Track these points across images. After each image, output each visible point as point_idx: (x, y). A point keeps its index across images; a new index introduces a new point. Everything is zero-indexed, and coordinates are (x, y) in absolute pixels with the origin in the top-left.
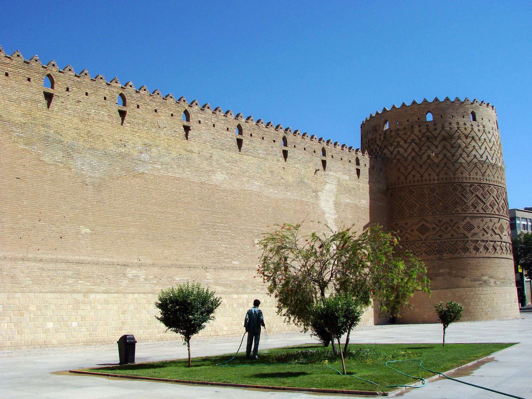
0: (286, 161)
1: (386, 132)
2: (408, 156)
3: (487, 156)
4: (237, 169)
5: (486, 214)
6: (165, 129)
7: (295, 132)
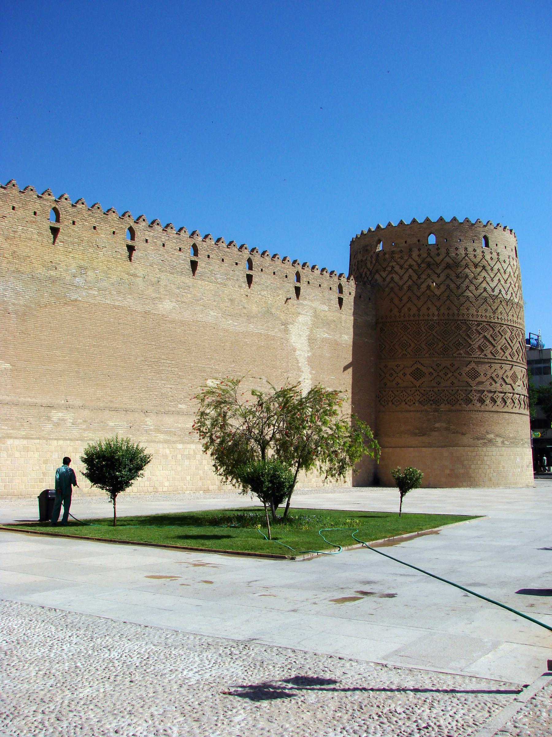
0: (249, 287)
3: (500, 290)
4: (189, 296)
5: (495, 359)
6: (105, 249)
7: (264, 253)
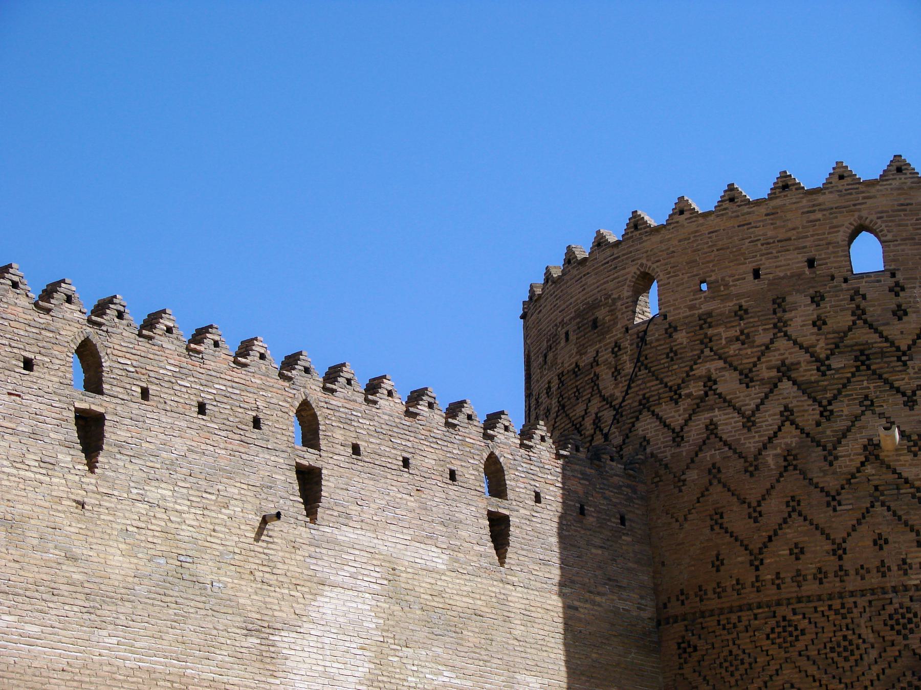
0: (92, 467)
1: (645, 332)
2: (765, 447)
